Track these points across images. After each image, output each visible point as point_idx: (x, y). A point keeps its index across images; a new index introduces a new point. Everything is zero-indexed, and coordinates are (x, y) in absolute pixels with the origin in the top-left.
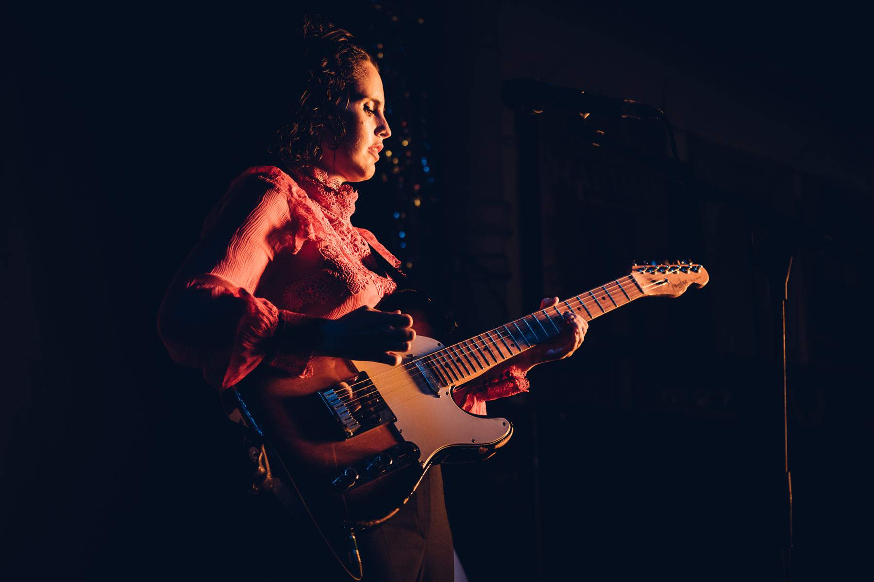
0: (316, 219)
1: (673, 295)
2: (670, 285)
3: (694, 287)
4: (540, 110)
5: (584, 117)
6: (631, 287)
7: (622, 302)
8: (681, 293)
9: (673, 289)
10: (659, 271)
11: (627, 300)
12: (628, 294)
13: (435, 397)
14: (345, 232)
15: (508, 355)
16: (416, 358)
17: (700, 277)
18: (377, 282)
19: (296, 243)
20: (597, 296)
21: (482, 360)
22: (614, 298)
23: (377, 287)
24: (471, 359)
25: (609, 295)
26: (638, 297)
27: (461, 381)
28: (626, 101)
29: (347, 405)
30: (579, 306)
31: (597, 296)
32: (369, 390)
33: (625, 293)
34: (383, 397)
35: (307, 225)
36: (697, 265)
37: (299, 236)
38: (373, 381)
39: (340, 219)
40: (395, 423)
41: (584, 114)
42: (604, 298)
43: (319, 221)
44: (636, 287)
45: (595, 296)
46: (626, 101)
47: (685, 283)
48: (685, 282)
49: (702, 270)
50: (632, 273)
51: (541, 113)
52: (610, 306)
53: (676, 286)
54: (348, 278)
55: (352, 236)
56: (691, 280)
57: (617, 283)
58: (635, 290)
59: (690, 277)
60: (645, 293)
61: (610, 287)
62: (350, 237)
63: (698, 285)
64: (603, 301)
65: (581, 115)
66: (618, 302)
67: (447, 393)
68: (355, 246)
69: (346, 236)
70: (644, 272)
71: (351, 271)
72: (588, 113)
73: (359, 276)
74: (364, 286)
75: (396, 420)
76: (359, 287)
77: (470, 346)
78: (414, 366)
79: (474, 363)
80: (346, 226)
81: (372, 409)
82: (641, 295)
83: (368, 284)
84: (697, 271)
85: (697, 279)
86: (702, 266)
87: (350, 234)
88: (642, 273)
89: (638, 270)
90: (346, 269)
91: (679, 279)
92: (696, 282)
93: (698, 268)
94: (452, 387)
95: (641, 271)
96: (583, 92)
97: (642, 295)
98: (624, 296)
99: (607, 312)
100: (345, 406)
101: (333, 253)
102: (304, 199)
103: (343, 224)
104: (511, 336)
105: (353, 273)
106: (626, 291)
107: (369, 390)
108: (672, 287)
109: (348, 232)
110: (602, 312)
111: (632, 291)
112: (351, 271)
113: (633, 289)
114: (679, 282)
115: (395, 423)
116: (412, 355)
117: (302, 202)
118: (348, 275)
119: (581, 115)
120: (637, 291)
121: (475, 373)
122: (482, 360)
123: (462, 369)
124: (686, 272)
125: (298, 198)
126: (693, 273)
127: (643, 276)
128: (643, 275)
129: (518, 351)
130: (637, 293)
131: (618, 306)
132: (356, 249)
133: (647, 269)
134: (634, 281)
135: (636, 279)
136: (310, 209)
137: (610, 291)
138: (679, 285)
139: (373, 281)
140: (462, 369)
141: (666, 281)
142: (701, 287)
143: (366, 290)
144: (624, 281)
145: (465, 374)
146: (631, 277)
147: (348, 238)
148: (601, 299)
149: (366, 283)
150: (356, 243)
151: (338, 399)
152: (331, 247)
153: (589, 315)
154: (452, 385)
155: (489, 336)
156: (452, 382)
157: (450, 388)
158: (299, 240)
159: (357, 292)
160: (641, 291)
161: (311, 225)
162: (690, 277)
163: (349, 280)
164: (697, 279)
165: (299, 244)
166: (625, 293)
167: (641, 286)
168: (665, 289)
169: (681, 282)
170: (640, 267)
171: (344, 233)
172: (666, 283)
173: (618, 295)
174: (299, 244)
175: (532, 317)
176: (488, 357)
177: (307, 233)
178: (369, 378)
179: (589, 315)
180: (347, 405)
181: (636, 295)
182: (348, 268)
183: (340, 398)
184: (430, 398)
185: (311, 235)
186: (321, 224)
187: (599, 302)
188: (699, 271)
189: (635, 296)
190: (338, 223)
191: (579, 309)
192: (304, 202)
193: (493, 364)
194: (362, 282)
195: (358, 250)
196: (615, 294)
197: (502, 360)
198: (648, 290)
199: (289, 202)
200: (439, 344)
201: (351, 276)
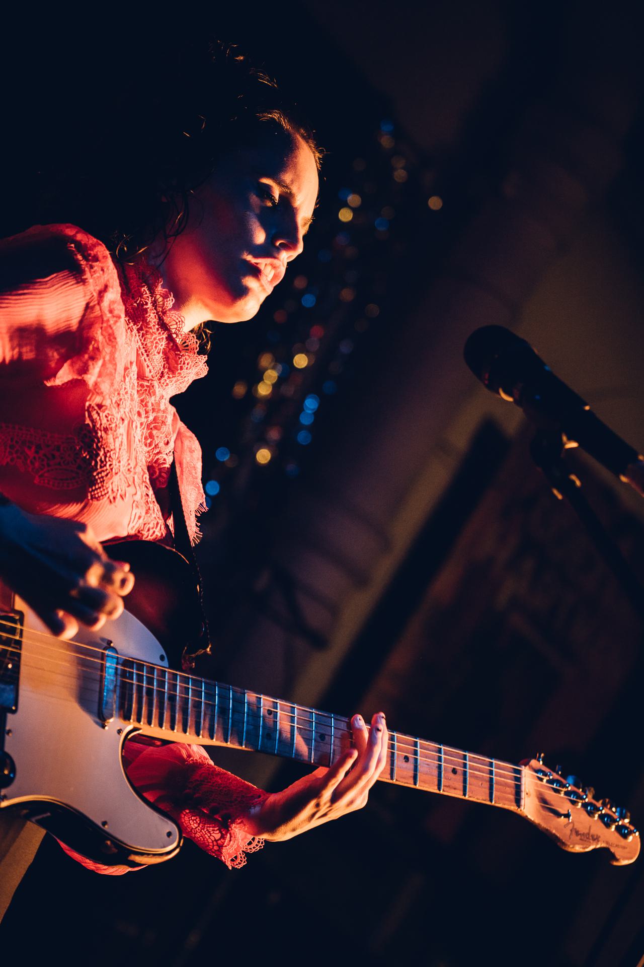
0: (114, 359)
1: (564, 844)
2: (571, 826)
3: (605, 855)
7: (477, 795)
8: (578, 849)
9: (571, 834)
10: (567, 793)
14: (150, 405)
17: (624, 848)
18: (137, 507)
19: (61, 373)
23: (134, 513)
25: (465, 773)
26: (506, 807)
31: (446, 761)
35: (93, 358)
36: (632, 828)
37: (72, 365)
39: (156, 383)
42: (454, 771)
43: (116, 364)
44: (513, 791)
47: (594, 840)
48: (596, 839)
49: (634, 839)
50: (523, 767)
53: (577, 833)
54: (99, 470)
55: (155, 419)
56: (607, 843)
57: (491, 765)
59: (608, 837)
60: (522, 808)
61: (476, 763)
62: (151, 418)
63: (613, 857)
64: (451, 775)
68: (151, 436)
69: (147, 412)
70: (545, 781)
71: (110, 465)
73: (116, 479)
74: (114, 498)
76: (105, 494)
80: (157, 399)
82: (513, 808)
83: (123, 499)
84: (625, 836)
85: (617, 846)
86: (637, 834)
87: (155, 414)
89: (537, 771)
90: (106, 457)
91: (590, 827)
92: (612, 850)
93: (631, 832)
95: (540, 775)
98: (487, 791)
99: (445, 793)
101: (104, 421)
102: (115, 319)
103: (154, 393)
105: (112, 469)
108: (571, 830)
109: (154, 410)
111: (505, 793)
112: (110, 465)
113: (508, 789)
114: (586, 831)
117: (108, 321)
118: (101, 467)
120: (512, 797)
124: (608, 826)
125: (107, 312)
126: (617, 835)
127: (537, 783)
128: (540, 782)
130: (507, 799)
132: (149, 441)
133: (551, 777)
134: (518, 779)
135: (524, 780)
136: (115, 338)
138: (583, 834)
139: (134, 502)
141: (567, 816)
142: (615, 864)
143: (113, 505)
144: (502, 769)
146: (519, 772)
147: (147, 417)
148: (450, 770)
149: (121, 496)
150: (155, 432)
152: (107, 412)
158: (68, 371)
159: (98, 499)
160: (518, 802)
161: (100, 363)
162: (608, 837)
163: (98, 474)
164: (617, 846)
165: (64, 375)
167: (523, 795)
168: (557, 826)
169: (588, 834)
170: (544, 768)
171: (146, 405)
172: (566, 819)
174: (64, 375)
177: (84, 370)
181: (507, 802)
182: (110, 456)
185: (89, 376)
186: (115, 370)
188: (631, 838)
190: (147, 386)
191: (406, 759)
192: (111, 322)
194: (115, 489)
195: (150, 445)
196: (477, 777)
198: (529, 809)
199: (88, 307)
201: (103, 471)
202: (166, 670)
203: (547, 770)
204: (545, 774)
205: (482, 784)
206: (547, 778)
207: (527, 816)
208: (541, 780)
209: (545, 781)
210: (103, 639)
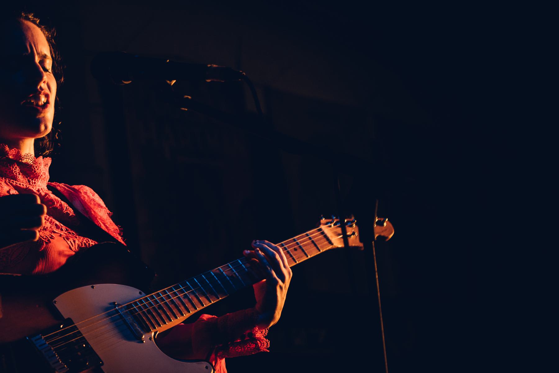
4: (128, 81)
5: (171, 84)
6: (320, 239)
7: (313, 253)
11: (318, 251)
12: (306, 252)
13: (139, 342)
15: (207, 303)
16: (119, 305)
17: (386, 230)
20: (289, 247)
21: (182, 308)
22: (319, 244)
24: (185, 301)
25: (300, 247)
26: (328, 249)
27: (164, 327)
28: (209, 66)
29: (55, 350)
30: (296, 247)
31: (289, 247)
32: (75, 336)
33: (315, 245)
34: (88, 342)
36: (382, 219)
38: (78, 327)
40: (102, 367)
41: (171, 81)
42: (295, 249)
44: (325, 239)
45: (287, 247)
46: (209, 66)
51: (131, 83)
52: (302, 257)
57: (307, 235)
58: (325, 242)
61: (302, 239)
63: (385, 238)
64: (295, 252)
65: (168, 82)
66: (309, 253)
67: (150, 339)
70: (332, 226)
72: (174, 80)
75: (103, 364)
77: (170, 294)
78: (229, 268)
79: (175, 311)
81: (79, 353)
82: (330, 247)
84: (382, 225)
85: (382, 232)
88: (330, 226)
89: (327, 224)
92: (382, 234)
94: (155, 333)
95: (329, 225)
96: (168, 61)
97: (332, 246)
98: (315, 248)
99: (300, 262)
100: (53, 351)
104: (200, 287)
106: (316, 243)
107: (75, 336)
110: (305, 257)
111: (322, 243)
115: (102, 367)
116: (115, 303)
119: (168, 82)
120: (326, 242)
121: (176, 320)
122: (182, 308)
123: (163, 316)
127: (330, 229)
129: (294, 262)
130: (326, 245)
131: (309, 257)
134: (323, 233)
137: (301, 242)
140: (163, 316)
142: (388, 240)
144: (313, 233)
145: (184, 311)
146: (320, 230)
148: (293, 250)
151: (46, 343)
153: (318, 248)
154: (155, 330)
155: (143, 303)
156: (155, 328)
157: (153, 334)
160: (330, 243)
164: (382, 232)
166: (315, 245)
167: (330, 238)
170: (328, 220)
173: (309, 247)
175: (218, 271)
176: (189, 305)
178: (74, 324)
179: (318, 248)
180: (55, 350)
181: (326, 247)
183: (47, 343)
184: (133, 344)
187: (291, 253)
188: (385, 224)
189: (325, 248)
193: (192, 312)
196: (305, 245)
197: (202, 308)
198: (337, 242)
200: (140, 293)
202: (147, 296)
203: (330, 220)
204: (331, 223)
205: (311, 246)
206: (333, 224)
207: (338, 247)
208: (330, 226)
209: (332, 226)
210: (110, 304)
